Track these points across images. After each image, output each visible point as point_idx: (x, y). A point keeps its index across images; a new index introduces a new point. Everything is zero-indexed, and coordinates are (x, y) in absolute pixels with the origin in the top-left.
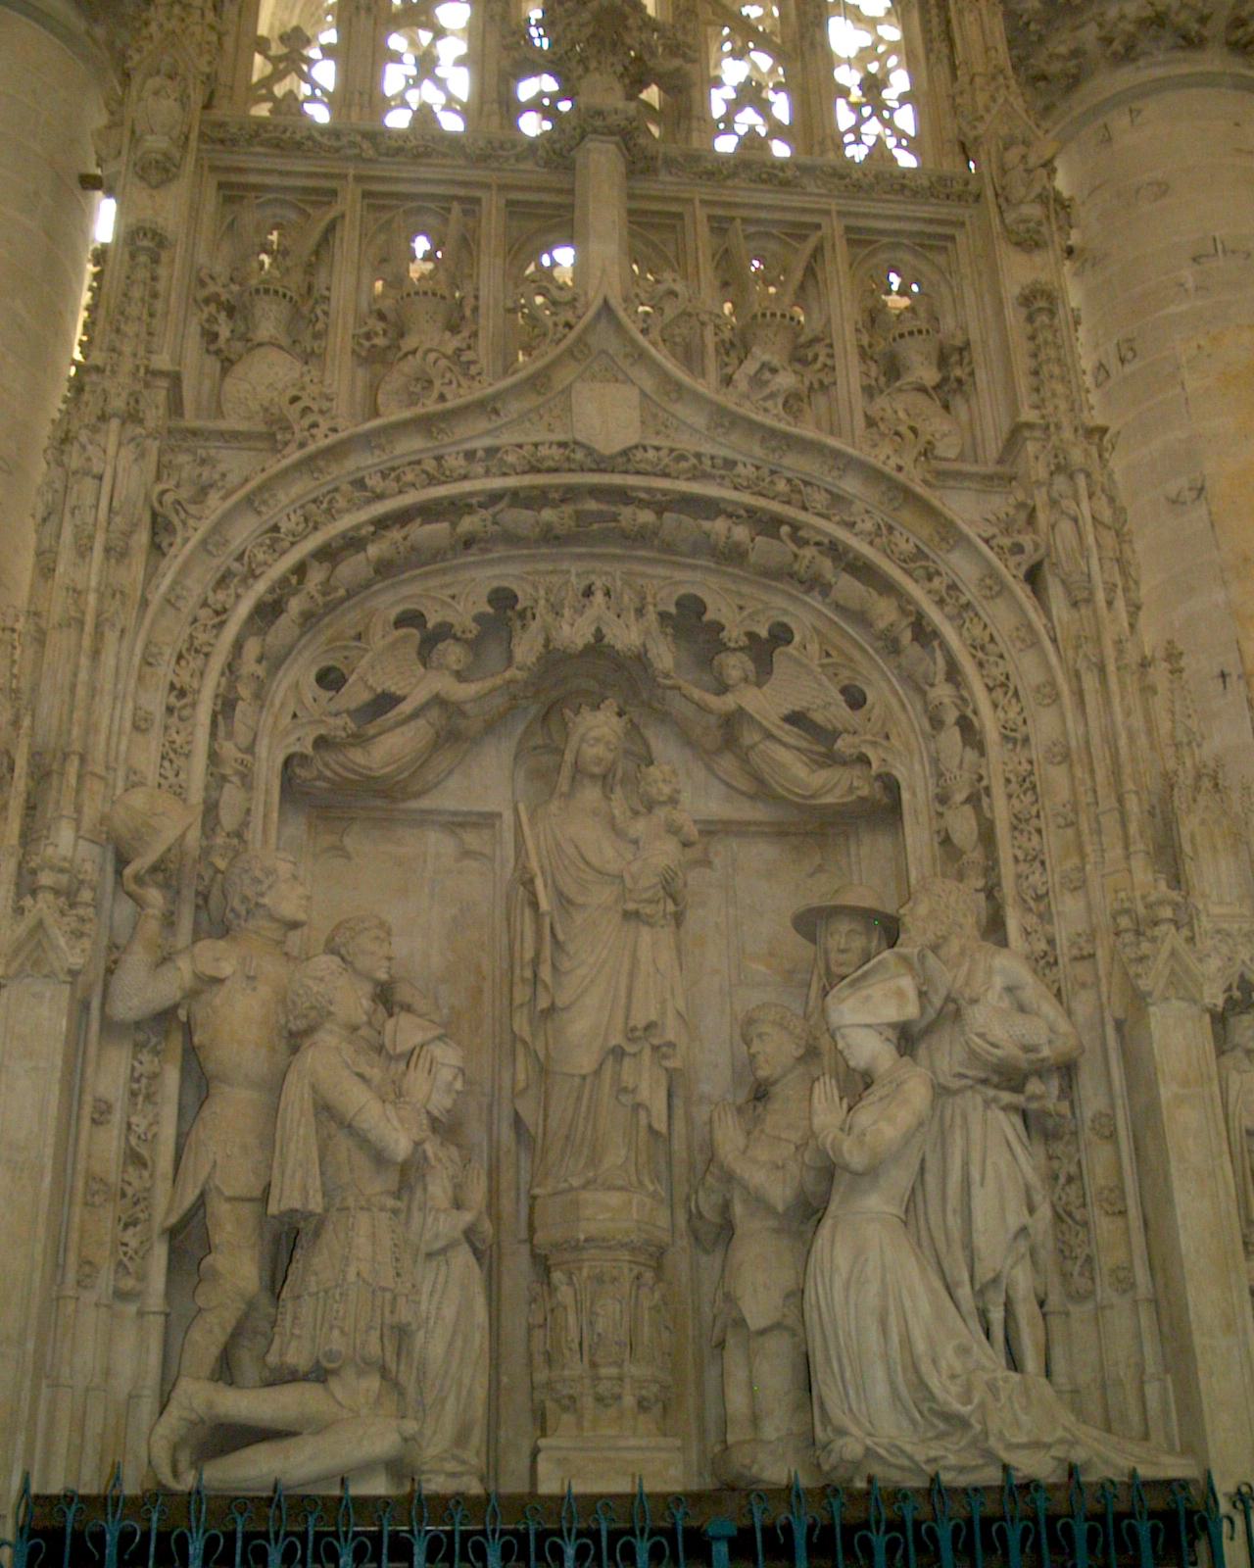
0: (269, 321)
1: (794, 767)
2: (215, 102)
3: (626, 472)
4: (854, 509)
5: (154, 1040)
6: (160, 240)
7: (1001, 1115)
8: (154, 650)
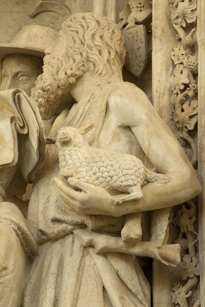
7: (100, 261)
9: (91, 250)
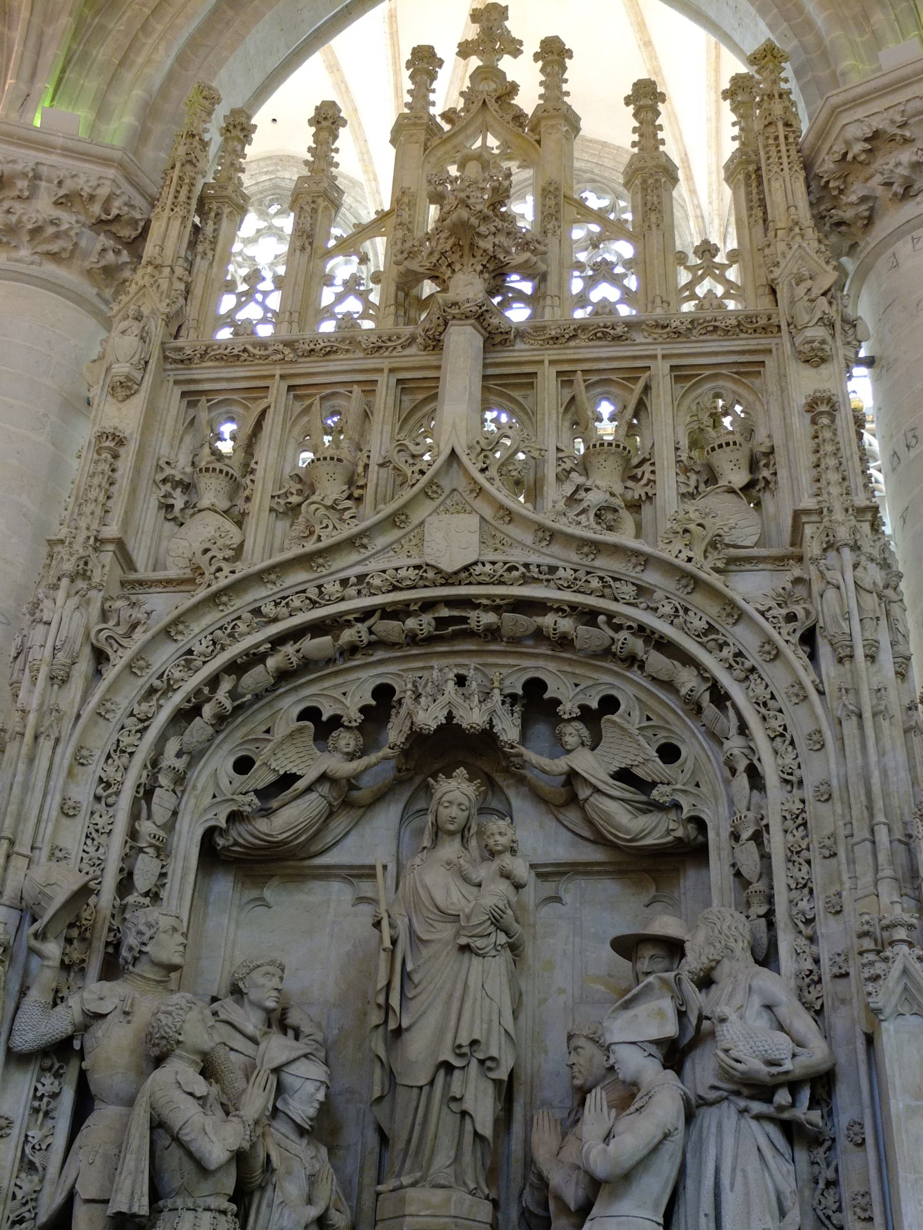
0: (211, 492)
1: (621, 816)
2: (183, 332)
3: (470, 583)
4: (655, 596)
5: (57, 1066)
6: (121, 442)
7: (754, 1124)
8: (85, 752)
9: (746, 1114)
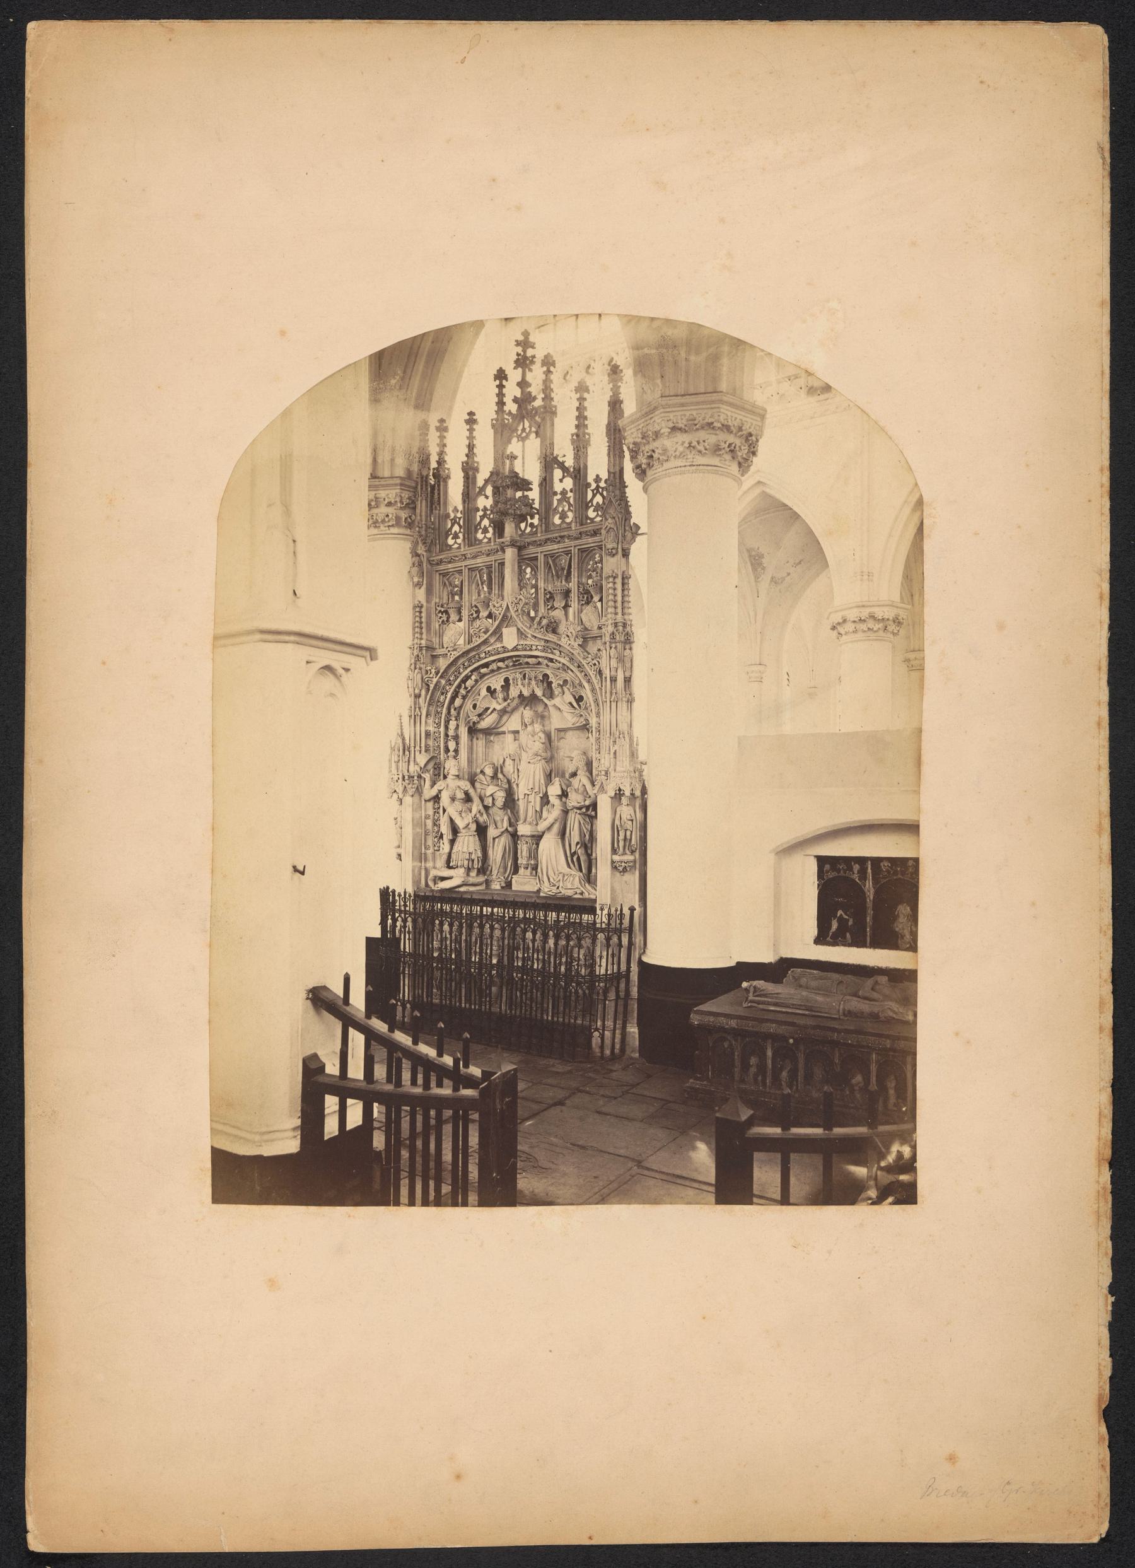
7: (578, 816)
